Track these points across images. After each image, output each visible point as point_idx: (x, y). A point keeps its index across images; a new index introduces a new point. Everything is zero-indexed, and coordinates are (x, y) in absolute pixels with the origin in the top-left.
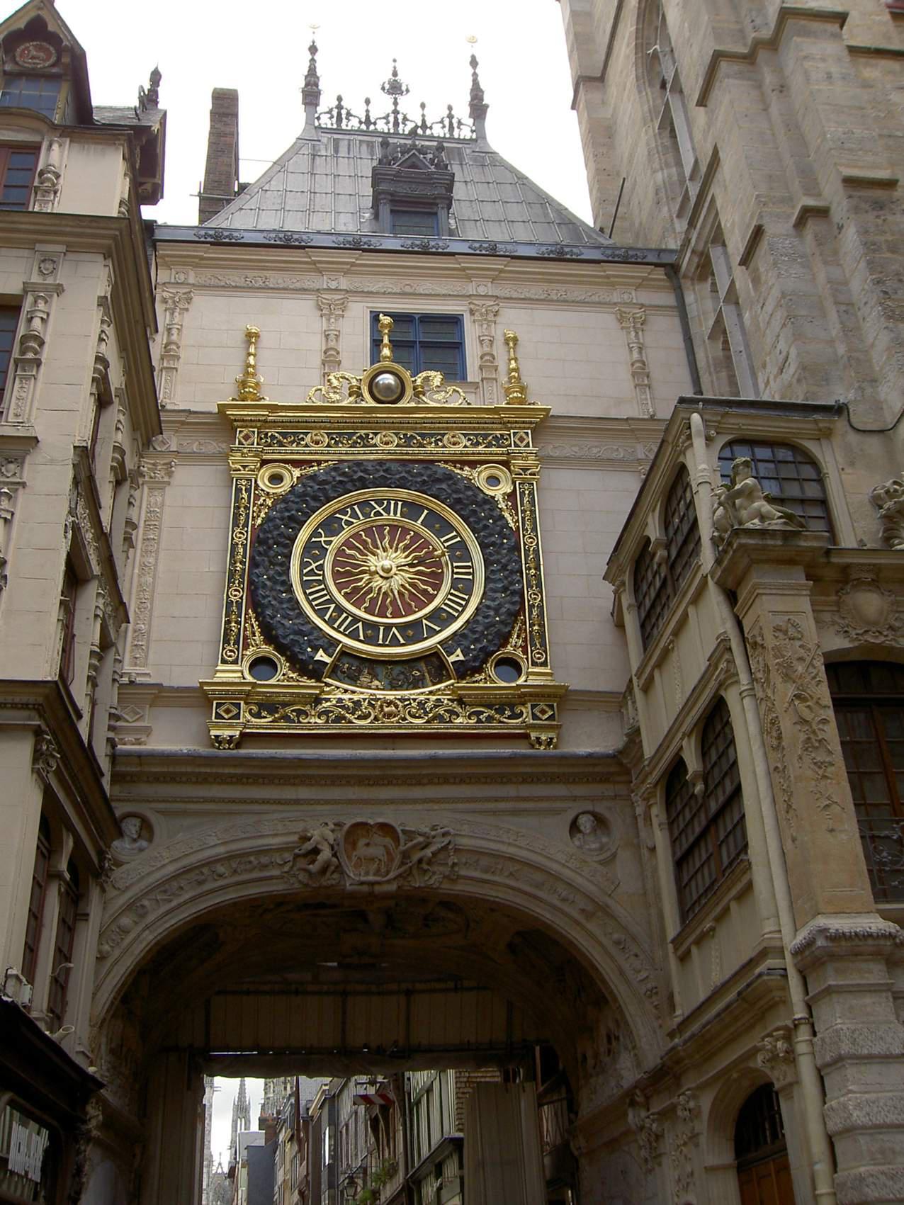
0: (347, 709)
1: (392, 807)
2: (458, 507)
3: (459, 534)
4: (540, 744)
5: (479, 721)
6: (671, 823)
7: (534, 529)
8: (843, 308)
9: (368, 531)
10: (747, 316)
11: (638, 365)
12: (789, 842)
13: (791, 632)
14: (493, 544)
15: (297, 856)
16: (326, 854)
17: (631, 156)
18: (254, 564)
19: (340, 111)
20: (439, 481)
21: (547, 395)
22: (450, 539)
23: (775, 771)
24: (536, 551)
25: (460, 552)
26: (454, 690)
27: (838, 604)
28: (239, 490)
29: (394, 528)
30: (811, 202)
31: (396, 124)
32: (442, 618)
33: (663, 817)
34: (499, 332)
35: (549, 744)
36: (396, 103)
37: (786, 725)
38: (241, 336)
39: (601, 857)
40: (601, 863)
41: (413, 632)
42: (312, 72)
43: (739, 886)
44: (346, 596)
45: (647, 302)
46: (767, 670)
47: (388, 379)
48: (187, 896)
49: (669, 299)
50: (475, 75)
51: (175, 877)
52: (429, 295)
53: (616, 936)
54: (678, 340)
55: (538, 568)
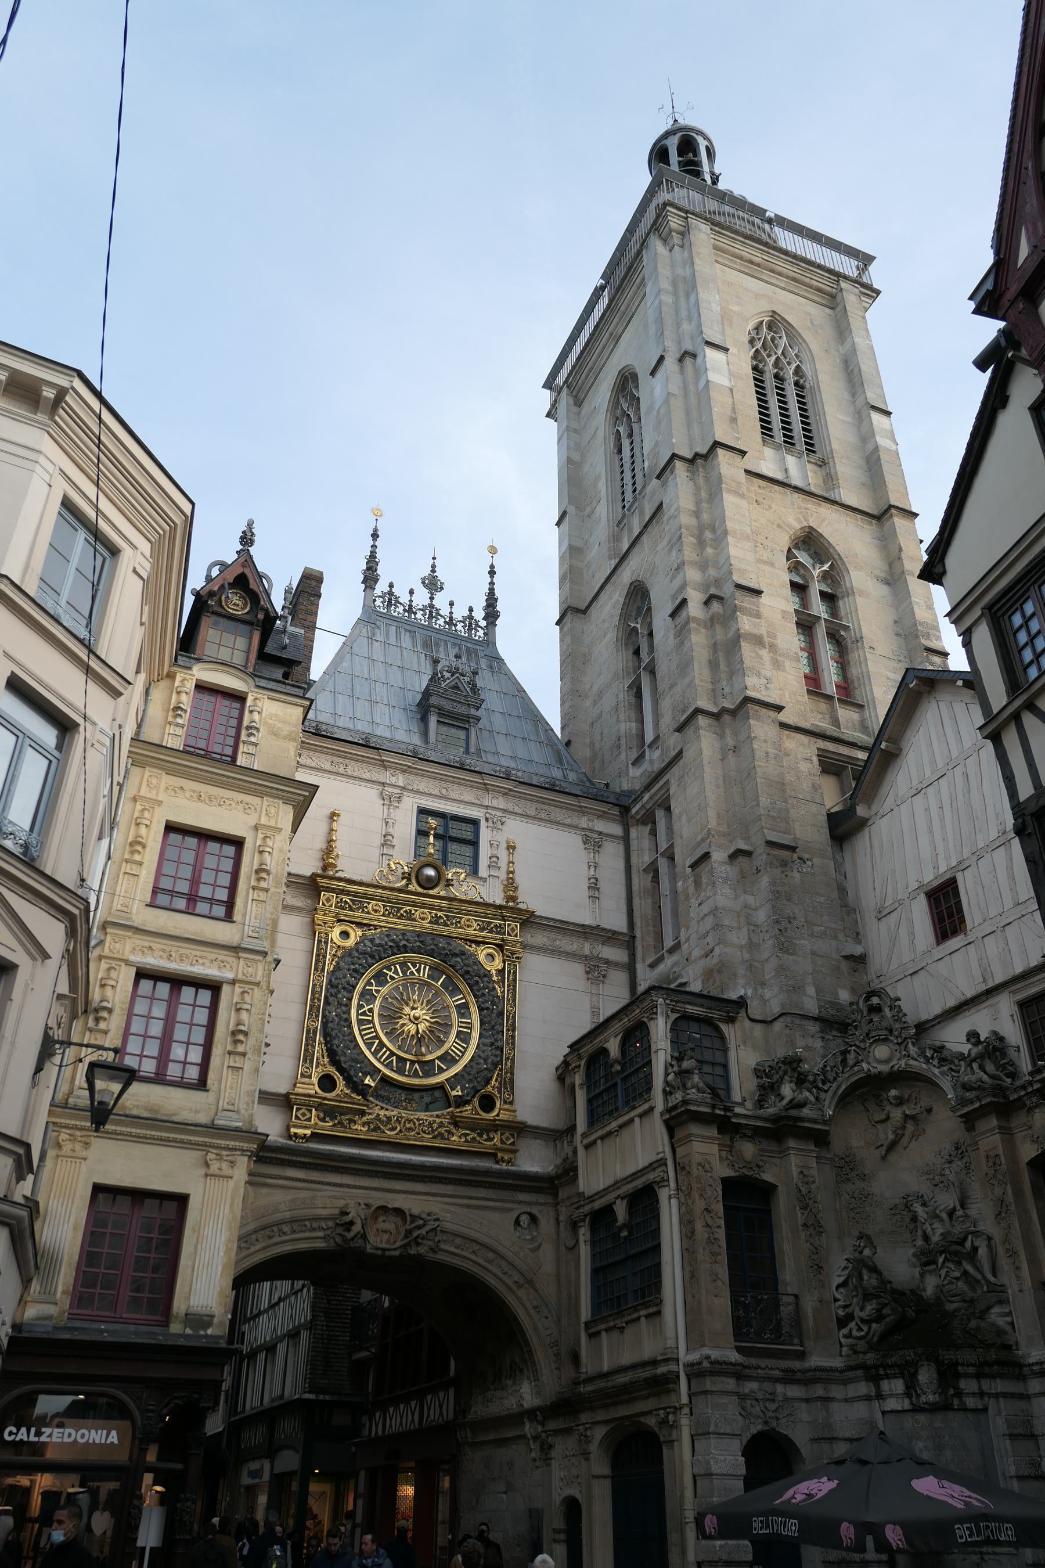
0: (382, 1122)
1: (403, 1196)
2: (467, 977)
3: (464, 997)
4: (503, 1162)
5: (467, 1141)
6: (593, 1243)
7: (514, 1001)
8: (752, 928)
9: (405, 986)
10: (680, 884)
11: (593, 880)
12: (689, 1298)
13: (707, 1165)
14: (487, 1009)
15: (337, 1224)
16: (357, 1228)
17: (600, 695)
18: (327, 1002)
19: (391, 599)
20: (456, 955)
21: (534, 898)
22: (459, 999)
23: (688, 1252)
24: (514, 1017)
25: (463, 1009)
26: (452, 1116)
27: (731, 1147)
28: (319, 941)
29: (423, 984)
30: (744, 847)
31: (431, 616)
32: (448, 1059)
33: (588, 1235)
34: (502, 837)
35: (508, 1162)
36: (432, 598)
37: (699, 1226)
38: (328, 812)
39: (531, 1246)
40: (531, 1250)
41: (428, 1067)
42: (373, 556)
43: (651, 1310)
44: (386, 1034)
45: (605, 831)
46: (690, 1188)
47: (431, 872)
48: (258, 1247)
49: (617, 830)
50: (492, 583)
51: (255, 1232)
52: (460, 801)
53: (535, 1303)
54: (621, 865)
55: (514, 1031)
